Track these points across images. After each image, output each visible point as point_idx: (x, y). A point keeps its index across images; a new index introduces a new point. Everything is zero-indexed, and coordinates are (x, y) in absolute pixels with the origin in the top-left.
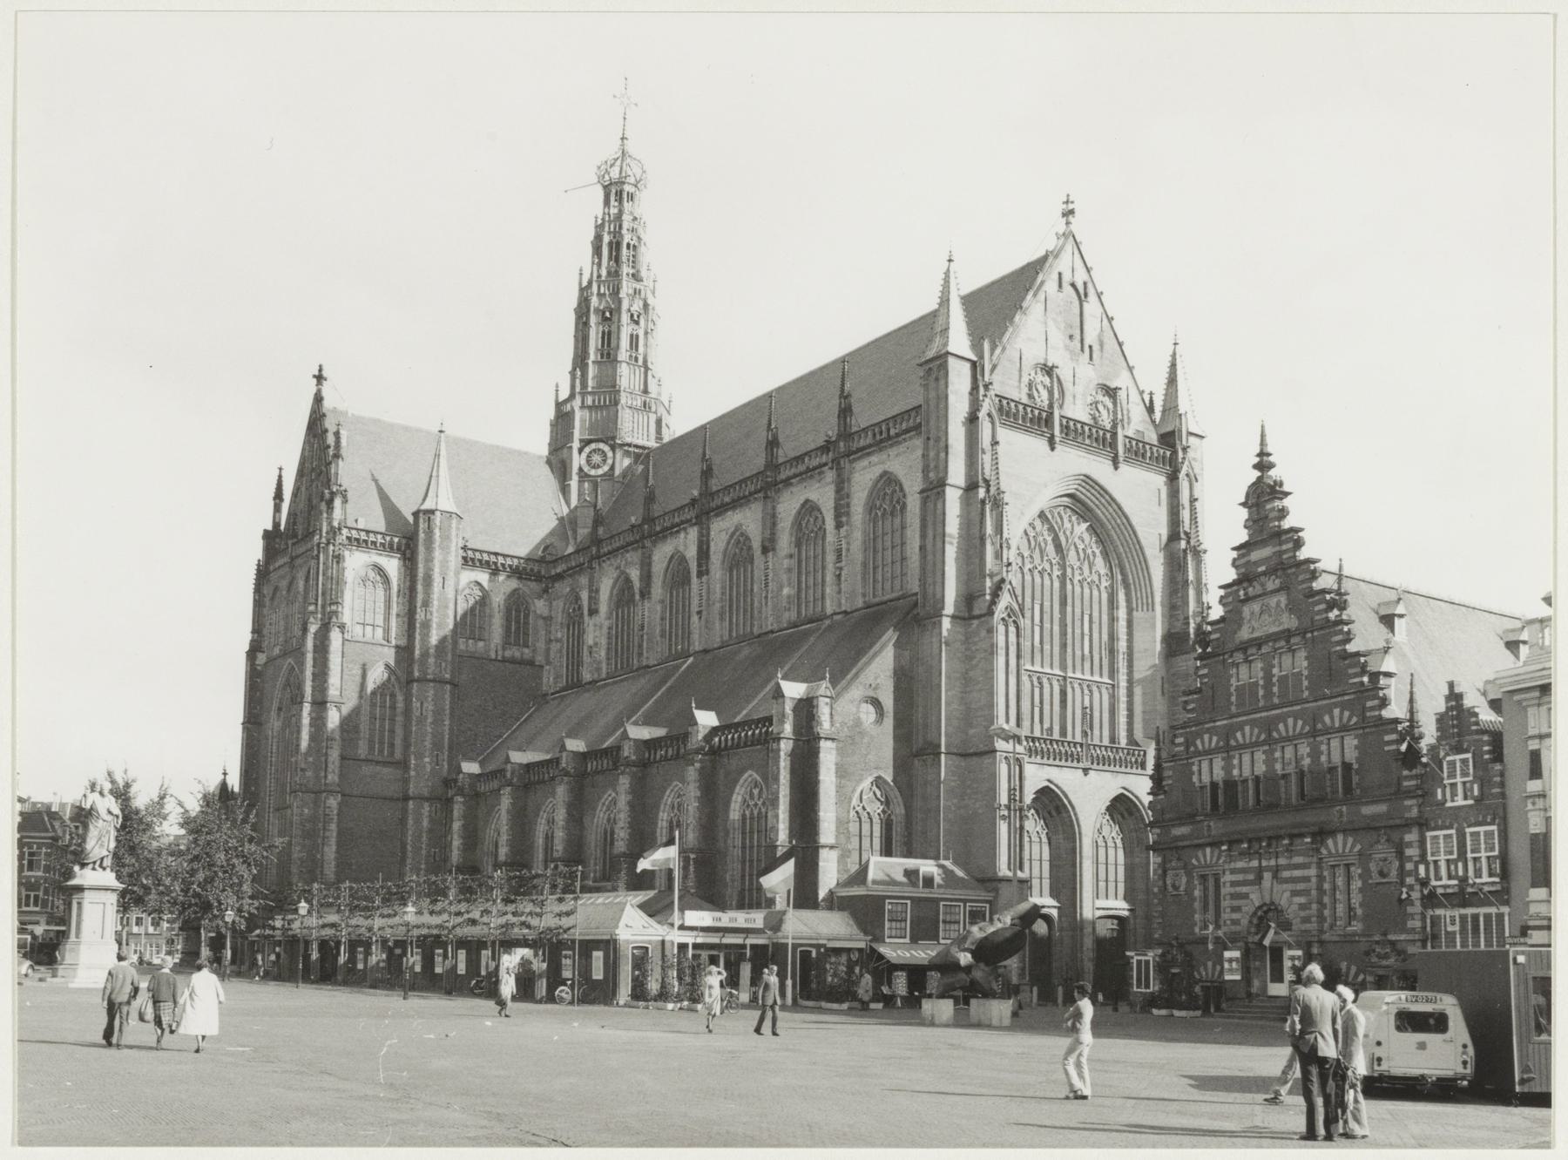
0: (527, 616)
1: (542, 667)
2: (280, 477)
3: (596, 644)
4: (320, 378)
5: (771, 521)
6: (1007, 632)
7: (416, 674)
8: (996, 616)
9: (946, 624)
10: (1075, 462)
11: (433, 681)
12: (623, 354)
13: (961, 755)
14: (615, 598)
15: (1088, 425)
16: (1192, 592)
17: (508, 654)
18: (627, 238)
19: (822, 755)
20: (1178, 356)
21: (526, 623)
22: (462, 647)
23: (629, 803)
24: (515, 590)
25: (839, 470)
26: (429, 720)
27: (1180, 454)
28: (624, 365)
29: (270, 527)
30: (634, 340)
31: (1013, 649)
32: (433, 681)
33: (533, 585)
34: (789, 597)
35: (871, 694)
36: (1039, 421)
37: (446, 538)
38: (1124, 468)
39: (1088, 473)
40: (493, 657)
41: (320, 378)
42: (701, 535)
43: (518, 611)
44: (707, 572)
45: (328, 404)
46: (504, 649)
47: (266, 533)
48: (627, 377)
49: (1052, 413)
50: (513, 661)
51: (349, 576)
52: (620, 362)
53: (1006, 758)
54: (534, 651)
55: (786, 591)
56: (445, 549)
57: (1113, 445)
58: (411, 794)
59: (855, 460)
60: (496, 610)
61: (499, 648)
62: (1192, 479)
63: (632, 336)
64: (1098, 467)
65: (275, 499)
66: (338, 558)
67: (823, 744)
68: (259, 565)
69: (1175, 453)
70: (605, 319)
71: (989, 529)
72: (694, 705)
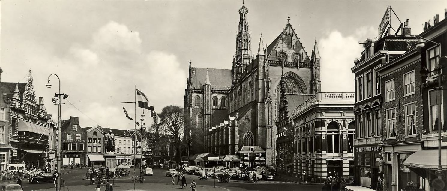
3: (233, 106)
4: (190, 62)
5: (247, 84)
9: (259, 104)
10: (287, 70)
11: (207, 115)
12: (243, 48)
17: (222, 108)
21: (225, 101)
22: (213, 108)
27: (313, 64)
30: (245, 44)
32: (207, 115)
35: (247, 117)
36: (279, 64)
37: (208, 89)
41: (190, 62)
50: (222, 109)
54: (226, 107)
55: (248, 97)
56: (208, 91)
59: (254, 73)
67: (235, 127)
71: (266, 87)
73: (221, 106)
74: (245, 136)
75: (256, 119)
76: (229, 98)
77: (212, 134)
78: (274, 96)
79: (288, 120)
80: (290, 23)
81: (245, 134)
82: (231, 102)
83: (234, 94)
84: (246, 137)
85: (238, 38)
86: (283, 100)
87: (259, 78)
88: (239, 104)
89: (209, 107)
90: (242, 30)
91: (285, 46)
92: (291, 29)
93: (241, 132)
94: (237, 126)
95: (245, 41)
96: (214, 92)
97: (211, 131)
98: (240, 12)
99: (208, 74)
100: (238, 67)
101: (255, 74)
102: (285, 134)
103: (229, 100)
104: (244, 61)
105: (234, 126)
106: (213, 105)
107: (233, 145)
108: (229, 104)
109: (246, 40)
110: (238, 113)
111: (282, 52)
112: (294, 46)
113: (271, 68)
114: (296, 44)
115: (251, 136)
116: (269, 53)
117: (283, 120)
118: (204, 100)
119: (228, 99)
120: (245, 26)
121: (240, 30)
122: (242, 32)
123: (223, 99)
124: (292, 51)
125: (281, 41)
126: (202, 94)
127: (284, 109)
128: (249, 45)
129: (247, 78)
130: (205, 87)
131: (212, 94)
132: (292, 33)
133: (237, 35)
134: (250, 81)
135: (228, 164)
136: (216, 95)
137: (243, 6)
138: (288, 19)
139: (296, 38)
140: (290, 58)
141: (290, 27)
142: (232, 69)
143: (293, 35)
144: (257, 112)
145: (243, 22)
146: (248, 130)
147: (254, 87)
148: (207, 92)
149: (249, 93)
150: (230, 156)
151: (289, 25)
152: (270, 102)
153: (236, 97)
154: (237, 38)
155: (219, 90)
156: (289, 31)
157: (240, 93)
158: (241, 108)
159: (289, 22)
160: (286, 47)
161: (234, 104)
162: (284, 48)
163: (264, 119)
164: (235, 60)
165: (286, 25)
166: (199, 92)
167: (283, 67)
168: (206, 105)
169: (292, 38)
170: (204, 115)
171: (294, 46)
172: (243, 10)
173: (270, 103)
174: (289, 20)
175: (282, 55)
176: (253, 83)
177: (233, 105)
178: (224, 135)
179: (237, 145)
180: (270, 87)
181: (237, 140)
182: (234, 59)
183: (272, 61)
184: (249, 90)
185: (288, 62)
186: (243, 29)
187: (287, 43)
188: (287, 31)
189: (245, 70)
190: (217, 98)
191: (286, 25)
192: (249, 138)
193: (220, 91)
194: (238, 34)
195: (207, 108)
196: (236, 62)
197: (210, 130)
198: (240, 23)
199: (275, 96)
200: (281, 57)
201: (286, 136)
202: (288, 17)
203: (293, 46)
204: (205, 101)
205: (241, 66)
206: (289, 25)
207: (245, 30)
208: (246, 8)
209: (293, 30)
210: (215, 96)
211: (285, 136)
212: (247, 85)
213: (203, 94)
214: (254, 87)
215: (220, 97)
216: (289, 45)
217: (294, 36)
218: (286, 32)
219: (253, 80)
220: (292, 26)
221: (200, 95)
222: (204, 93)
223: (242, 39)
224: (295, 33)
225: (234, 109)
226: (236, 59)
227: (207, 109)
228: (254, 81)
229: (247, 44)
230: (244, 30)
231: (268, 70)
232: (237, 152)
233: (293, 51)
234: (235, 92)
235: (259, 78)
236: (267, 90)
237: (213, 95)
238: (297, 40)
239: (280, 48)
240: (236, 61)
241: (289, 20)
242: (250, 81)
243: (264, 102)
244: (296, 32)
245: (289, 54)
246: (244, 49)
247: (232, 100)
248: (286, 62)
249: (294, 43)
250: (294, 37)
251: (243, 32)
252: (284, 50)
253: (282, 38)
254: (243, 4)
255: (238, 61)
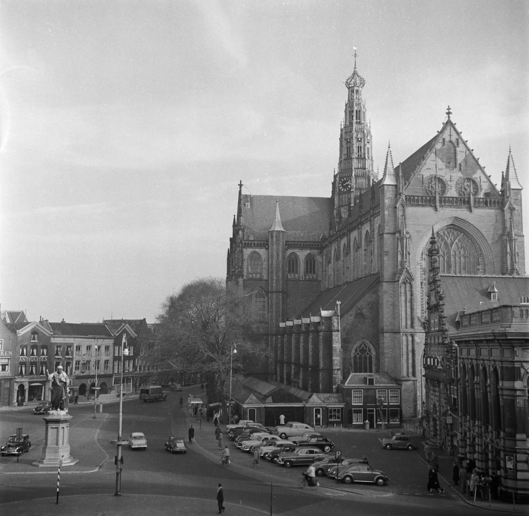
0: (314, 263)
1: (320, 281)
2: (234, 218)
3: (331, 275)
6: (405, 288)
7: (270, 290)
8: (400, 282)
12: (355, 155)
13: (393, 333)
14: (336, 258)
15: (455, 198)
16: (509, 257)
17: (307, 277)
18: (355, 108)
19: (333, 337)
20: (510, 157)
22: (289, 277)
23: (303, 346)
24: (309, 254)
25: (370, 221)
26: (274, 306)
28: (355, 159)
29: (232, 237)
30: (359, 148)
31: (408, 293)
33: (316, 251)
34: (365, 265)
35: (359, 312)
38: (476, 211)
39: (456, 216)
40: (301, 279)
42: (347, 239)
43: (311, 261)
44: (350, 252)
45: (243, 193)
46: (305, 276)
47: (231, 238)
48: (355, 164)
49: (436, 197)
50: (309, 280)
51: (246, 257)
52: (354, 158)
53: (405, 334)
54: (317, 275)
57: (469, 202)
58: (269, 333)
59: (376, 217)
60: (302, 262)
61: (303, 276)
62: (512, 209)
63: (358, 147)
64: (462, 213)
65: (233, 226)
66: (242, 252)
67: (334, 333)
68: (228, 250)
69: (503, 200)
70: (348, 142)
71: (400, 249)
72: (310, 315)
73: (307, 272)
74: (356, 350)
75: (378, 313)
76: (324, 257)
77: (286, 336)
78: (419, 267)
79: (445, 335)
80: (451, 119)
81: (355, 347)
82: (328, 266)
83: (335, 251)
84: (358, 354)
85: (343, 135)
86: (434, 289)
87: (386, 232)
88: (344, 274)
89: (281, 276)
90: (353, 120)
91: (441, 164)
92: (453, 132)
93: (345, 342)
94: (338, 331)
95: (358, 141)
96: (289, 245)
97: (283, 328)
98: (347, 84)
99: (278, 209)
100: (344, 193)
101: (376, 219)
102: (439, 365)
103: (324, 260)
104: (356, 180)
105: (330, 331)
106: (289, 272)
107: (330, 369)
108: (324, 269)
109: (361, 139)
110: (339, 303)
111: (435, 177)
112: (460, 164)
113: (410, 210)
114: (465, 161)
115: (370, 350)
116: (407, 178)
117: (435, 331)
118: (270, 262)
119: (323, 258)
120: (358, 112)
121: (348, 120)
122: (351, 124)
123: (310, 262)
124: (457, 175)
125: (433, 155)
126: (264, 250)
127: (438, 309)
128: (368, 149)
129: (362, 224)
130: (272, 234)
131: (287, 249)
132: (457, 140)
133: (342, 130)
134: (367, 231)
135: (318, 411)
136: (296, 251)
137: (355, 73)
138: (447, 111)
139: (464, 149)
140: (454, 189)
141: (452, 129)
142: (329, 195)
143: (458, 144)
144: (380, 301)
145: (355, 105)
146: (363, 338)
147: (376, 245)
148: (274, 246)
149: (365, 255)
150: (322, 396)
151: (449, 124)
152: (410, 279)
153: (337, 258)
154: (341, 135)
155: (301, 242)
156: (450, 135)
157: (347, 253)
158: (347, 283)
159: (449, 117)
160: (444, 167)
161: (334, 272)
162: (439, 169)
163: (395, 315)
164: (338, 179)
165: (443, 123)
166: (260, 246)
167: (438, 207)
168: (272, 272)
169: (457, 148)
170: (269, 293)
171: (460, 164)
172: (353, 80)
173: (409, 283)
174: (449, 113)
175: (435, 184)
176: (374, 238)
177: (332, 273)
178: (310, 346)
179: (338, 370)
180: (408, 250)
181: (337, 359)
182: (335, 177)
183: (414, 196)
184: (365, 250)
185: (448, 197)
186: (355, 118)
187: (445, 160)
188: (446, 135)
189: (358, 201)
190: (296, 257)
191: (443, 123)
192: (363, 356)
193: (304, 242)
194: (342, 127)
195: (275, 278)
196: (339, 183)
197: (282, 325)
198: (348, 106)
199: (421, 266)
200: (432, 187)
201: (441, 368)
202: (447, 108)
203: (458, 166)
204: (272, 264)
205: (349, 192)
206: (449, 124)
207: (359, 119)
208: (360, 77)
209: (458, 134)
210: (293, 253)
211: (440, 367)
212: (361, 238)
213: (267, 249)
214: (376, 245)
215: (302, 255)
216: (449, 163)
217: (461, 145)
218: (444, 137)
219: (373, 231)
220: (457, 127)
221: (262, 252)
222: (270, 248)
223: (352, 138)
224: (462, 139)
225: (334, 282)
226: (338, 177)
227: (274, 281)
228: (375, 233)
229: (362, 148)
230: (357, 119)
231: (404, 215)
232: (338, 386)
233: (460, 175)
234: (336, 247)
235: (386, 232)
236: (402, 255)
237: (289, 252)
238: (468, 152)
239: (430, 169)
240: (338, 181)
241: (449, 113)
242: (367, 231)
243: (396, 282)
244: (464, 137)
245: (451, 181)
246: (357, 156)
247: (329, 262)
248: (444, 197)
249: (460, 158)
250: (461, 148)
251: (354, 125)
252: (440, 173)
253: (434, 151)
254: (355, 68)
255: (344, 181)
